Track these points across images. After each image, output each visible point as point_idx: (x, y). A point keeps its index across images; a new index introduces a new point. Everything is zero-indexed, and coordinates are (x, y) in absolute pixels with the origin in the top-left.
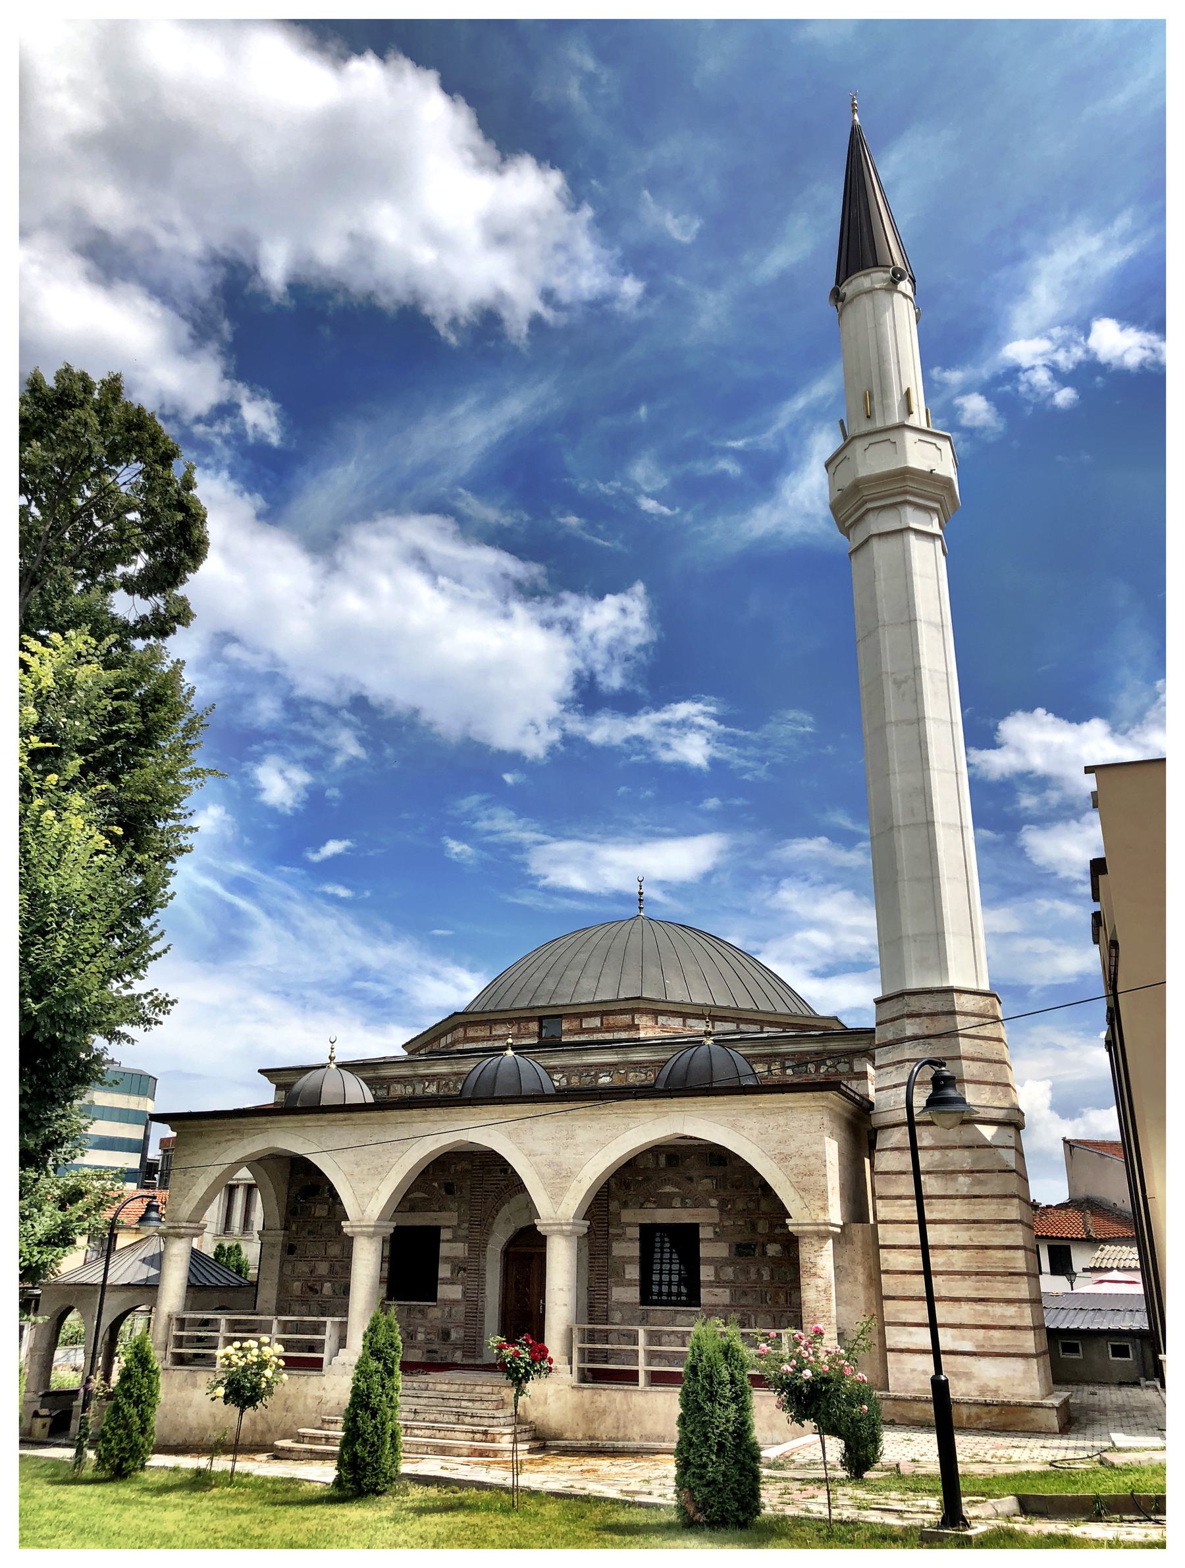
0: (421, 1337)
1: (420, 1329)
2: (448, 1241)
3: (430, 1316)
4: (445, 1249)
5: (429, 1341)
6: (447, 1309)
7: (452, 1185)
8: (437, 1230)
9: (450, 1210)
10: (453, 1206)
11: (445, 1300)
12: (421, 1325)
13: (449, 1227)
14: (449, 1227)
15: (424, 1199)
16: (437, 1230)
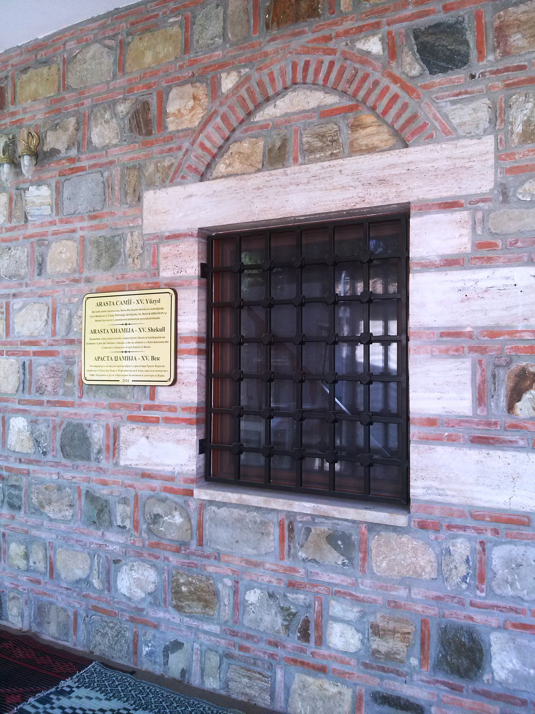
0: (342, 638)
1: (336, 608)
2: (451, 263)
3: (380, 564)
4: (432, 300)
5: (377, 662)
6: (461, 547)
7: (453, 30)
8: (394, 224)
9: (450, 133)
10: (473, 113)
11: (449, 509)
12: (340, 594)
13: (450, 205)
14: (450, 205)
15: (326, 113)
16: (394, 224)
